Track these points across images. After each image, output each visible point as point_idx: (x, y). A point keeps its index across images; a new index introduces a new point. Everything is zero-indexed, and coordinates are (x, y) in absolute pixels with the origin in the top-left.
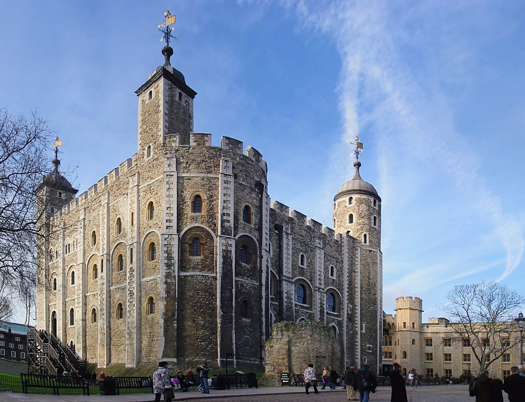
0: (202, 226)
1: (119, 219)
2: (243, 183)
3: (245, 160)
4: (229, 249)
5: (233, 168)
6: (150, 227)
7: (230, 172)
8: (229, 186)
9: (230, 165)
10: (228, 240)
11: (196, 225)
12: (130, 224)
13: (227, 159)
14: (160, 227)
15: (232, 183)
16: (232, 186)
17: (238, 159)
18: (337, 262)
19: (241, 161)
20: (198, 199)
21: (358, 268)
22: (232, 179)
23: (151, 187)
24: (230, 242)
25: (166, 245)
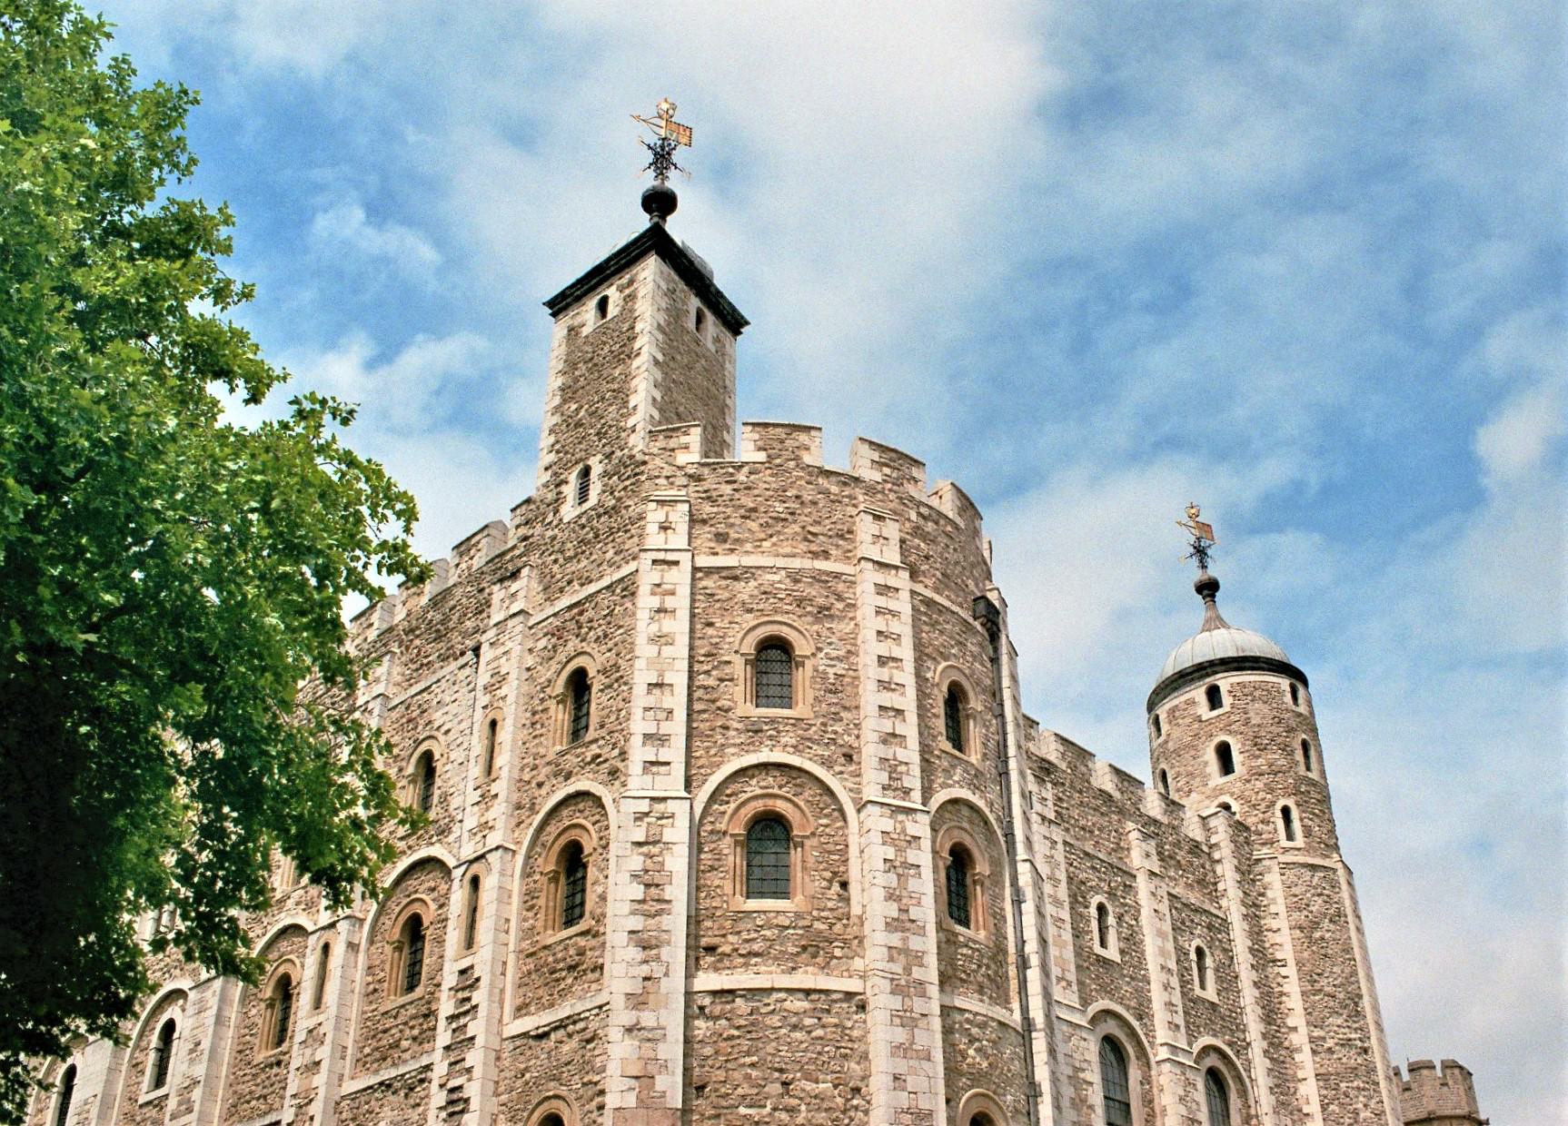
0: (795, 760)
1: (428, 758)
2: (938, 598)
3: (937, 523)
4: (912, 856)
5: (902, 541)
6: (568, 776)
7: (894, 557)
8: (893, 605)
9: (892, 530)
10: (901, 817)
11: (778, 756)
12: (476, 771)
13: (879, 510)
14: (614, 773)
15: (905, 595)
16: (903, 604)
17: (913, 516)
18: (1210, 927)
19: (921, 522)
20: (775, 654)
21: (1284, 943)
22: (902, 580)
23: (581, 613)
24: (912, 830)
25: (639, 844)
